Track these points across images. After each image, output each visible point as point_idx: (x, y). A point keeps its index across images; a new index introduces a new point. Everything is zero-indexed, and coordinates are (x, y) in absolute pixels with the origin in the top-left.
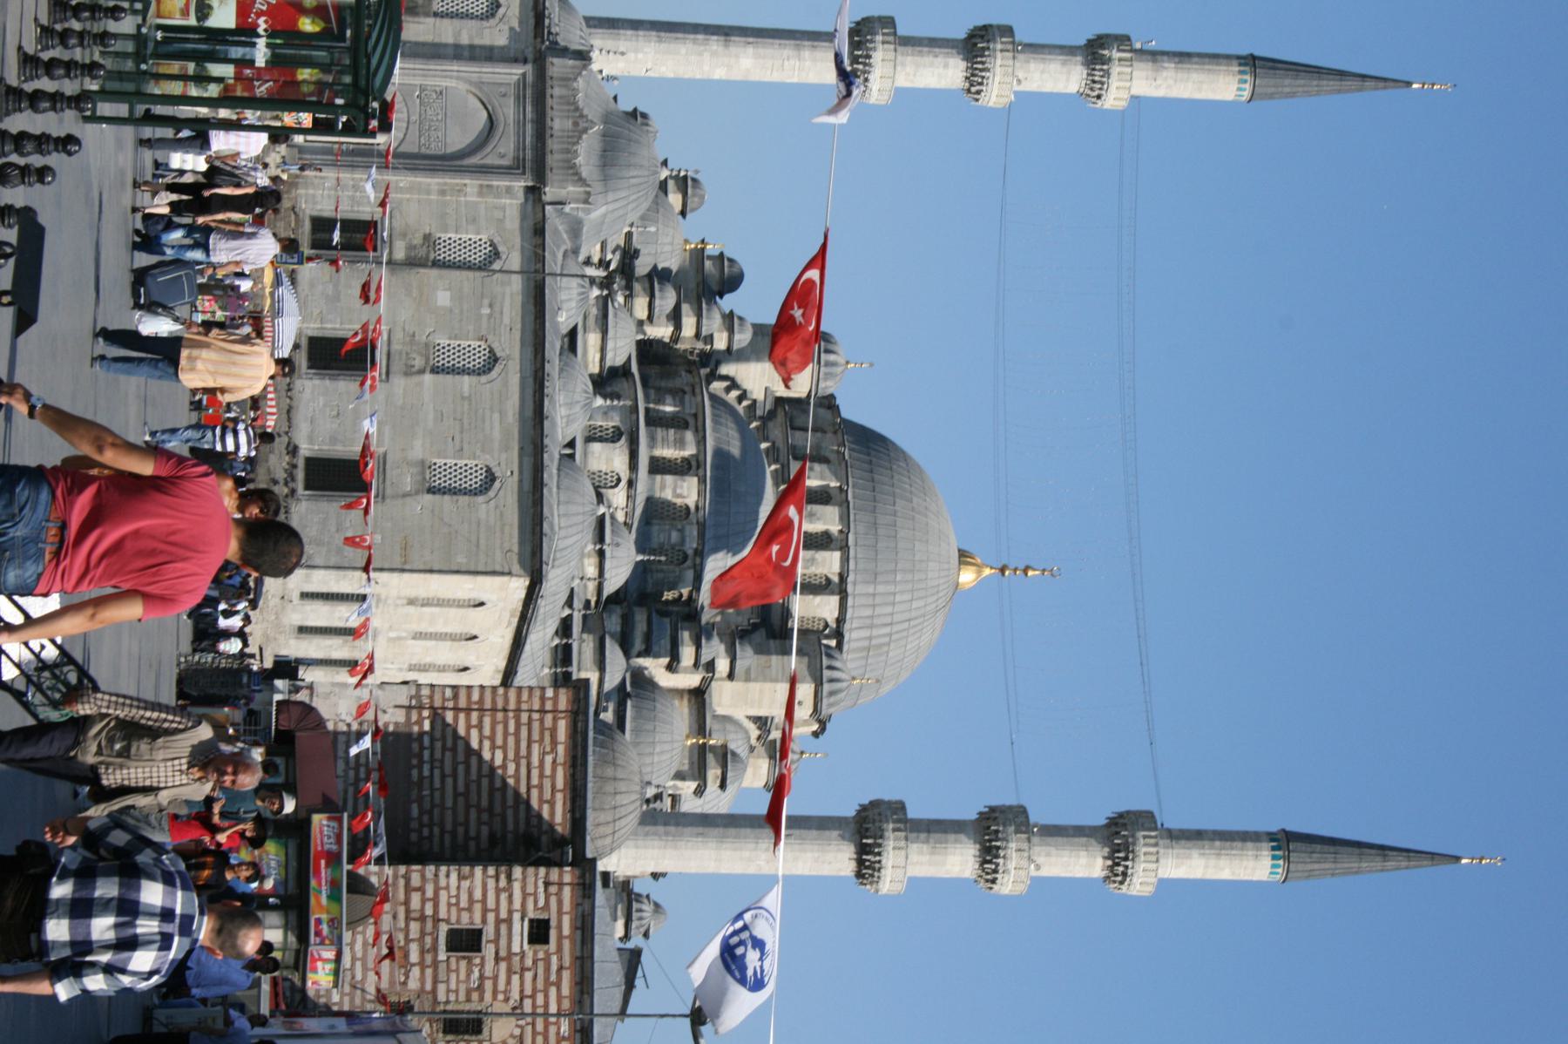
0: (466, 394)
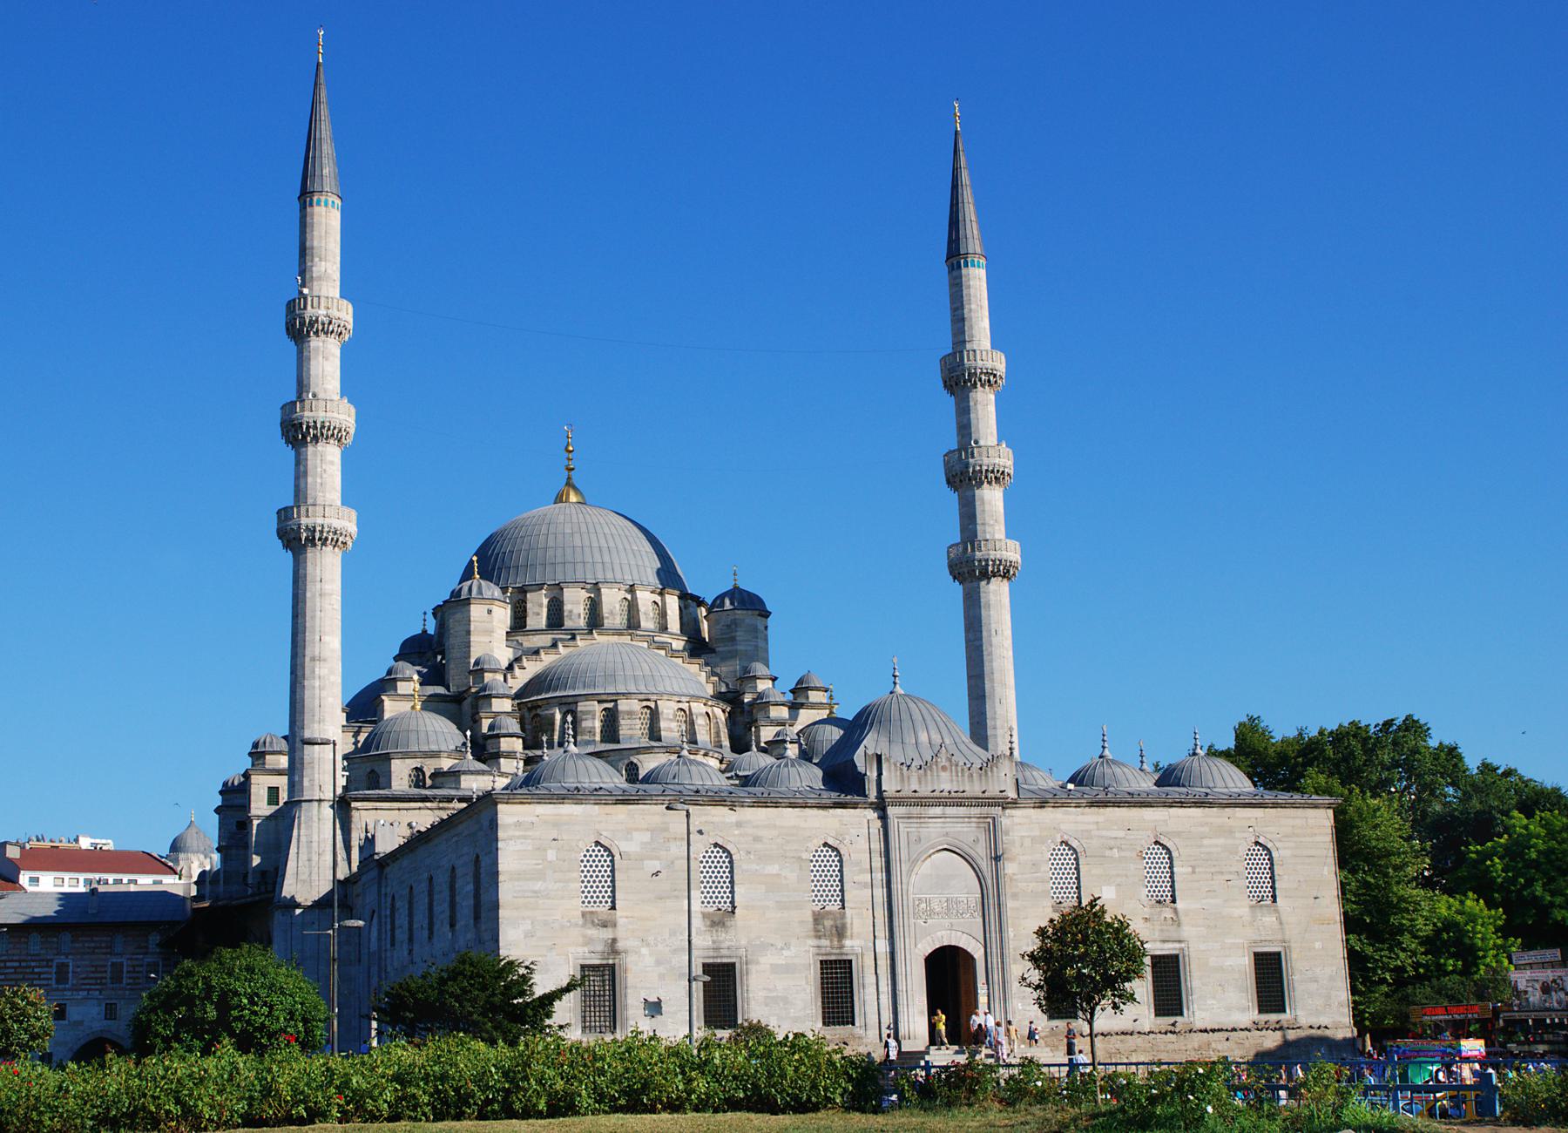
0: (1190, 869)
